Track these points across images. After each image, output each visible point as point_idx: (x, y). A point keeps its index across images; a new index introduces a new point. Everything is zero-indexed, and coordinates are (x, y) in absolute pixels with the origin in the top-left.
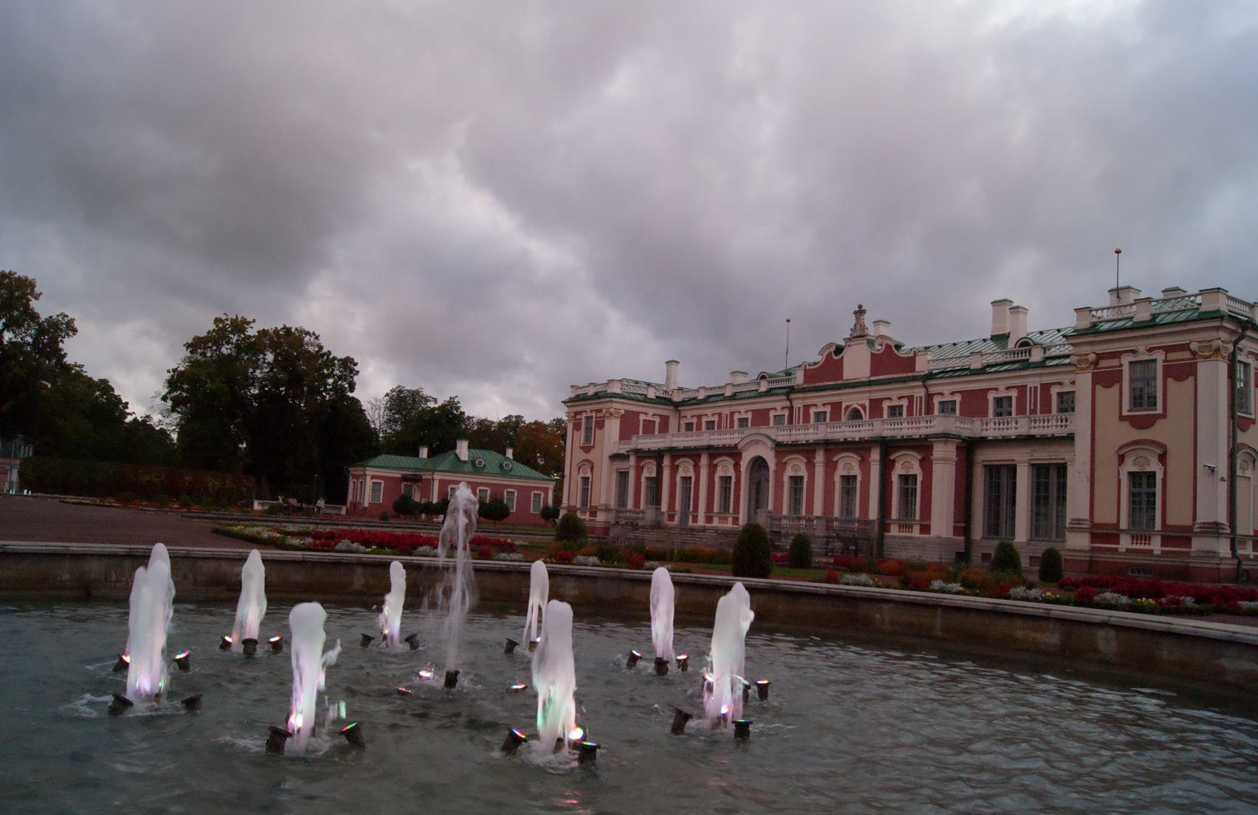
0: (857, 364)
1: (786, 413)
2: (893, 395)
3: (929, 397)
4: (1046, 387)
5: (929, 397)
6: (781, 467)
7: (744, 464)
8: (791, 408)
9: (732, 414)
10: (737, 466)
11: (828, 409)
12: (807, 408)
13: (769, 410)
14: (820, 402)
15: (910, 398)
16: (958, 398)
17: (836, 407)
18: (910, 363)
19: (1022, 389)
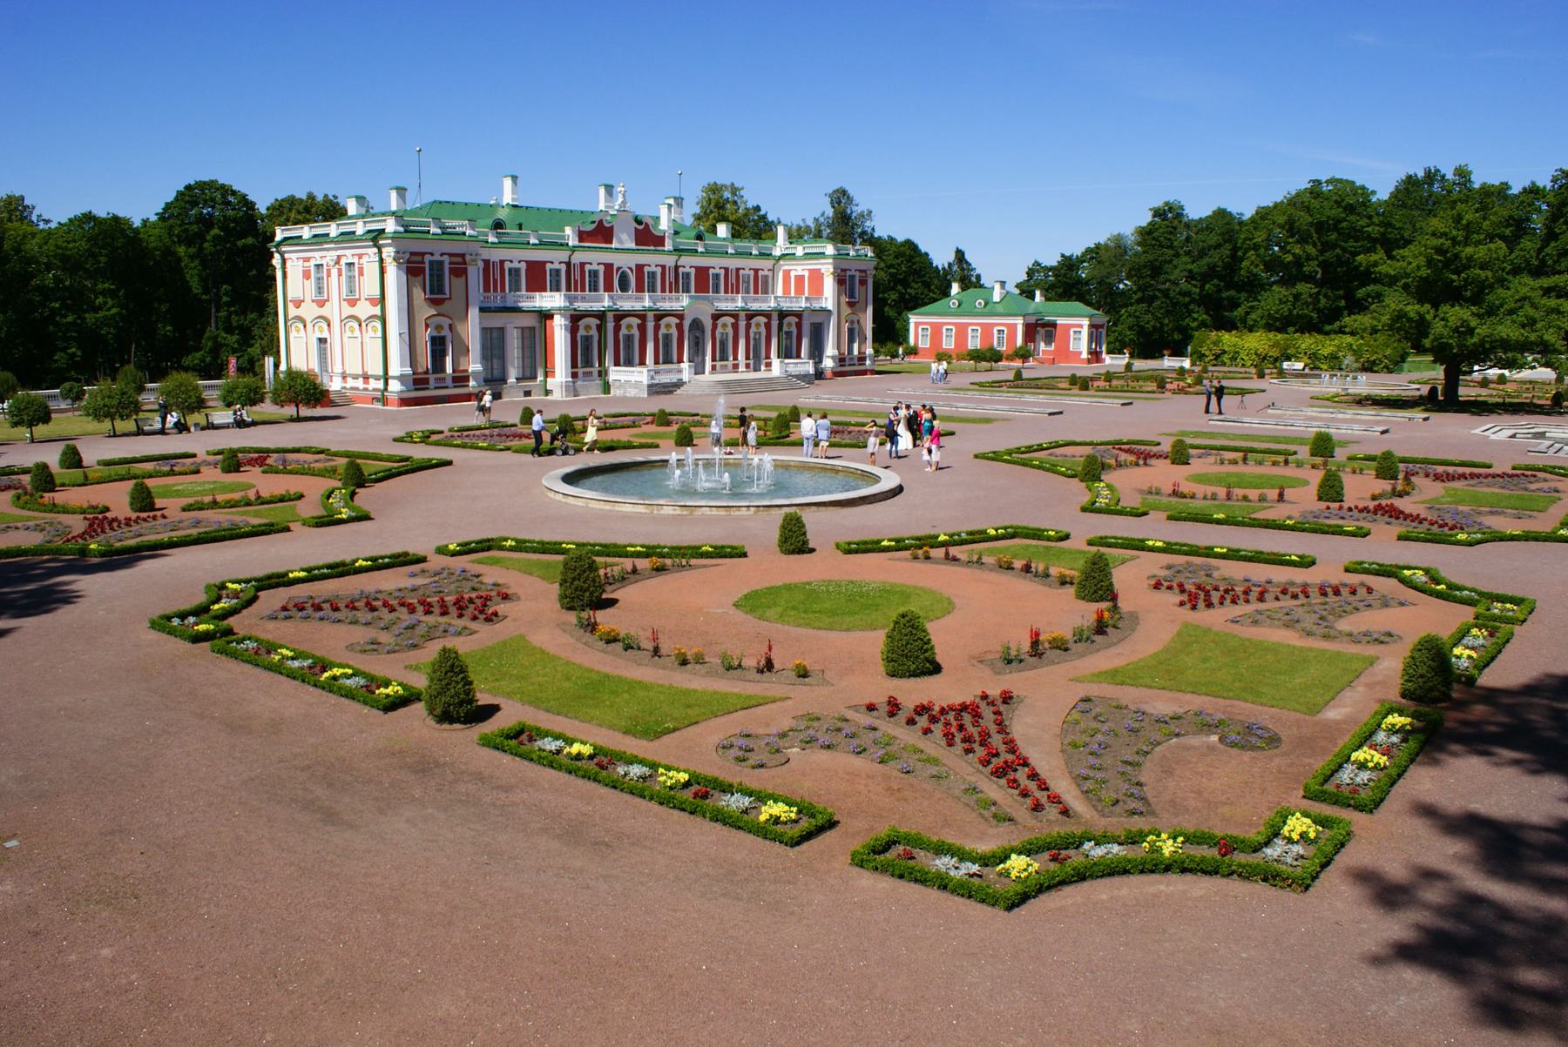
0: (624, 239)
1: (563, 268)
2: (652, 260)
3: (677, 267)
4: (738, 270)
5: (677, 267)
6: (714, 327)
7: (686, 324)
8: (568, 264)
9: (502, 262)
10: (680, 327)
11: (602, 268)
12: (582, 265)
13: (544, 263)
14: (594, 258)
15: (663, 267)
16: (693, 271)
17: (609, 267)
18: (660, 241)
19: (726, 270)
